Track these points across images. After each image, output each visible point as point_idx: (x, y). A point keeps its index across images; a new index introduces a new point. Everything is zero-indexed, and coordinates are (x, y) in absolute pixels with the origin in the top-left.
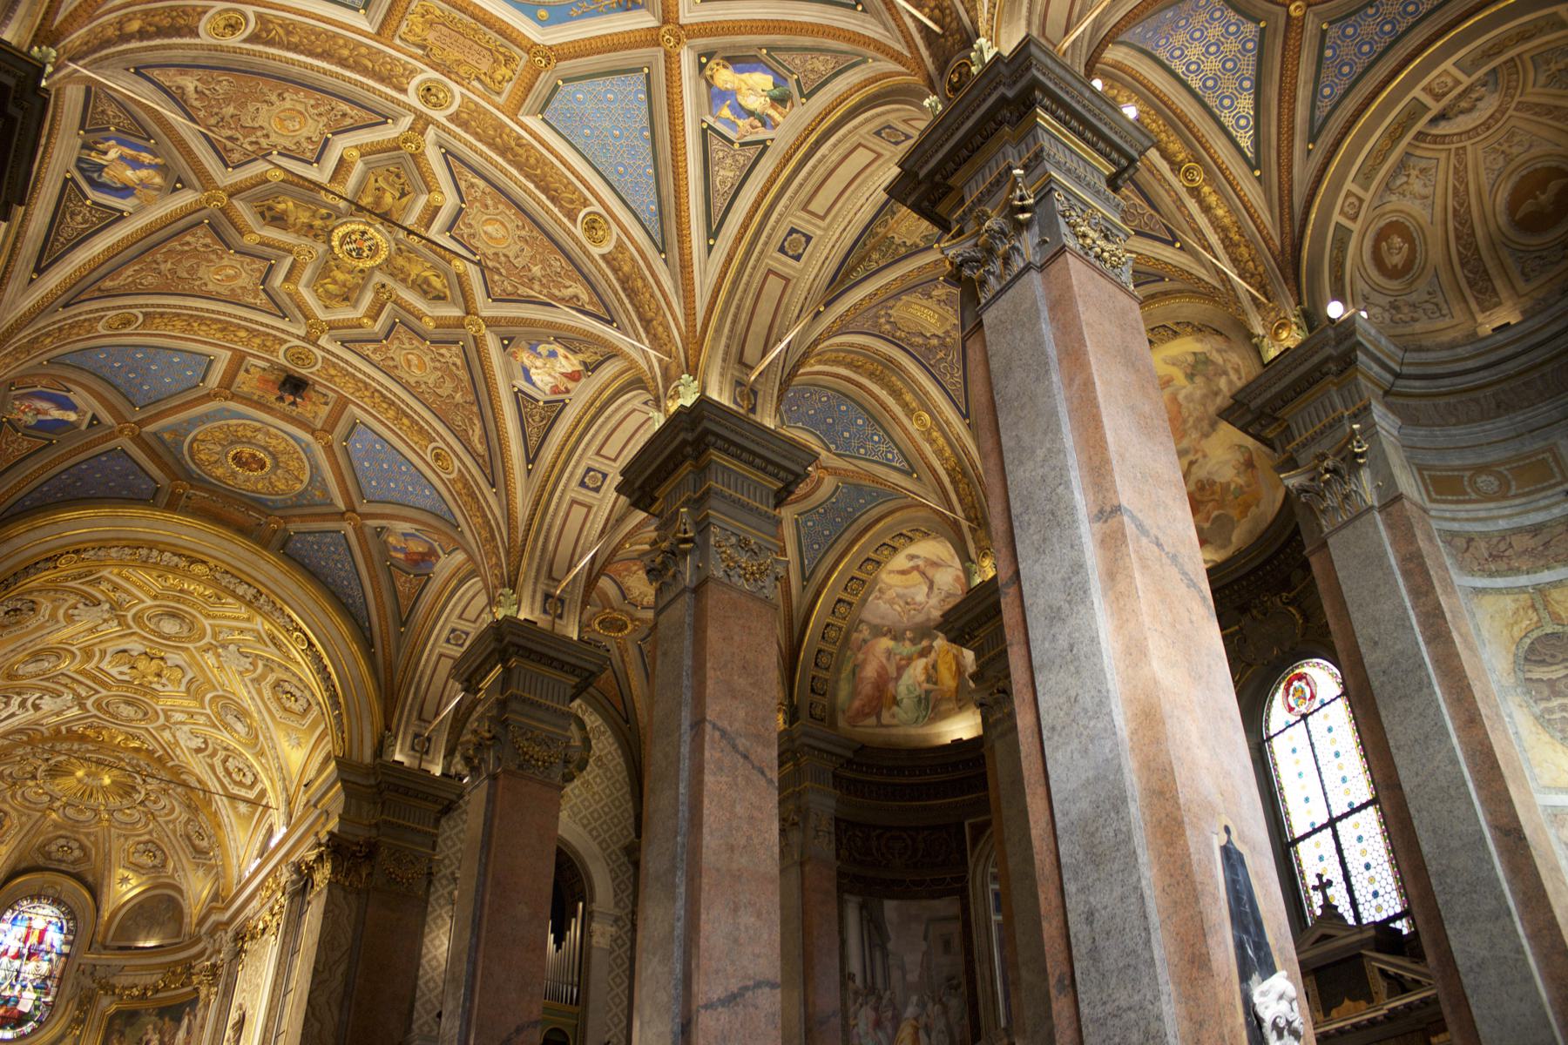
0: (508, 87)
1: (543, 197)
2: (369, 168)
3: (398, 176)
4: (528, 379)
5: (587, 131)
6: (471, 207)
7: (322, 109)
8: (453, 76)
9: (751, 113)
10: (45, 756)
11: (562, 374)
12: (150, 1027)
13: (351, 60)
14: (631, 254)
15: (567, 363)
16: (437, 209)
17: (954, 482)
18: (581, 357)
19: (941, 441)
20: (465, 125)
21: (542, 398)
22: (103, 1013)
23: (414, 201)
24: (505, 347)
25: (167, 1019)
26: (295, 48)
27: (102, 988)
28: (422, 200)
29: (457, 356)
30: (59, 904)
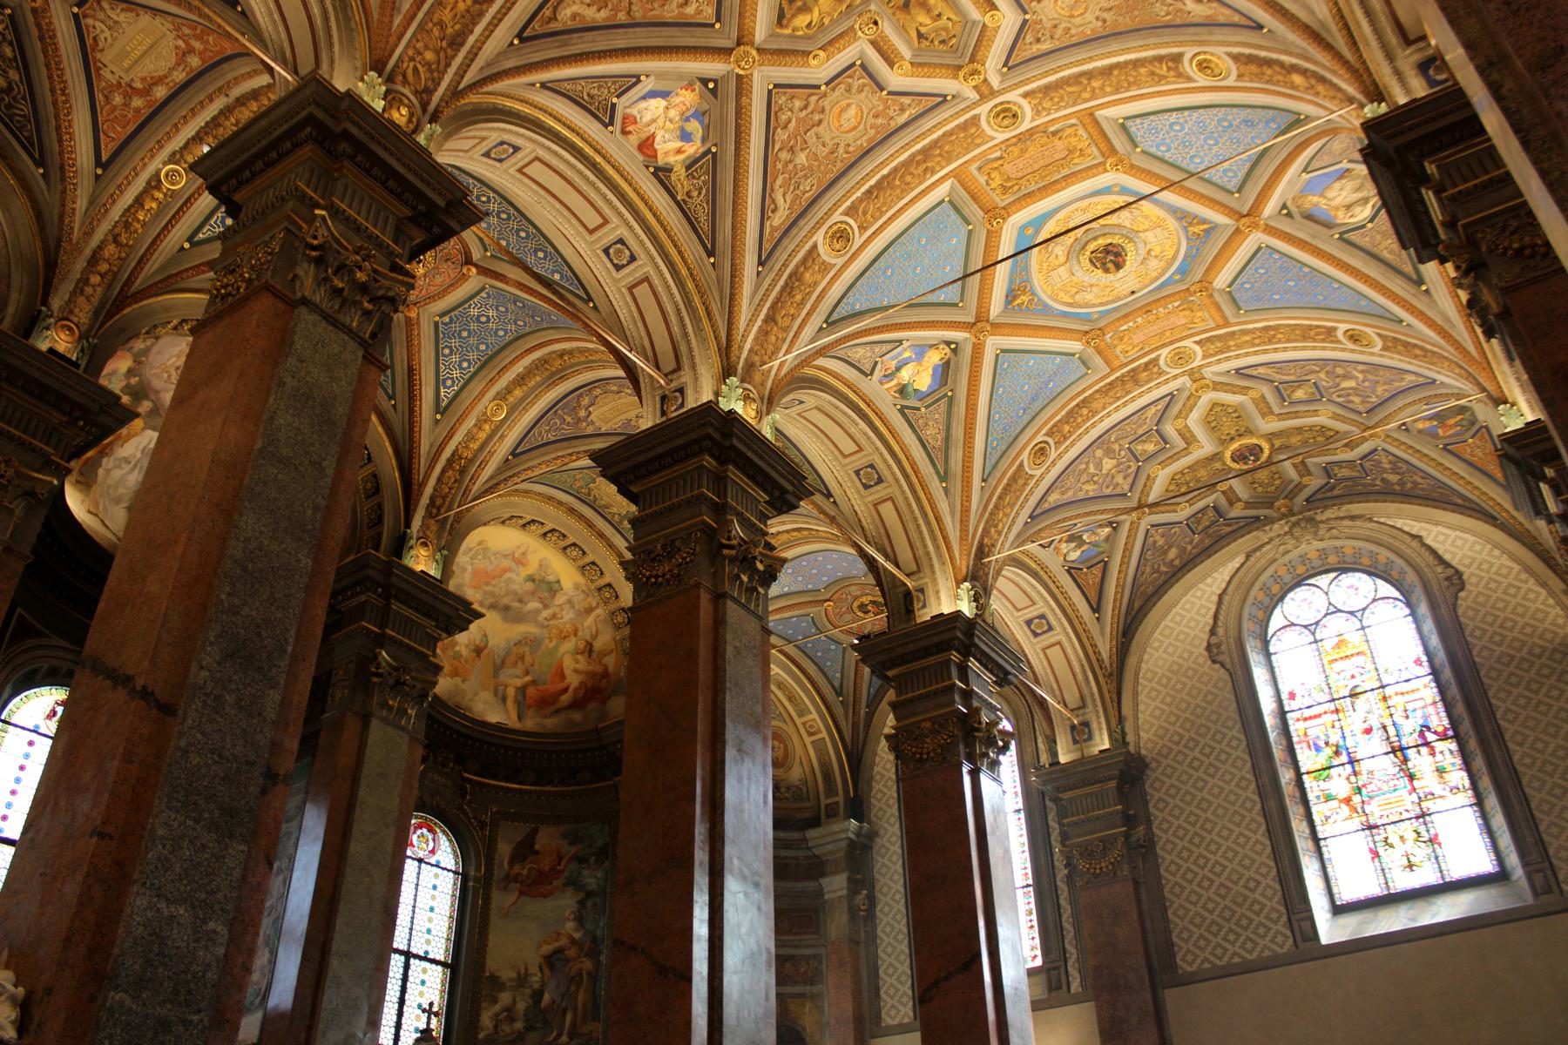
0: (982, 179)
1: (872, 182)
2: (966, 22)
3: (943, 42)
4: (653, 94)
5: (924, 241)
6: (880, 99)
7: (1059, 32)
8: (1014, 140)
9: (898, 369)
11: (653, 136)
13: (1085, 82)
14: (820, 282)
15: (669, 149)
16: (891, 64)
17: (450, 461)
18: (680, 172)
19: (482, 435)
20: (964, 127)
21: (621, 103)
23: (909, 43)
24: (705, 82)
26: (1137, 63)
28: (906, 53)
29: (699, 12)
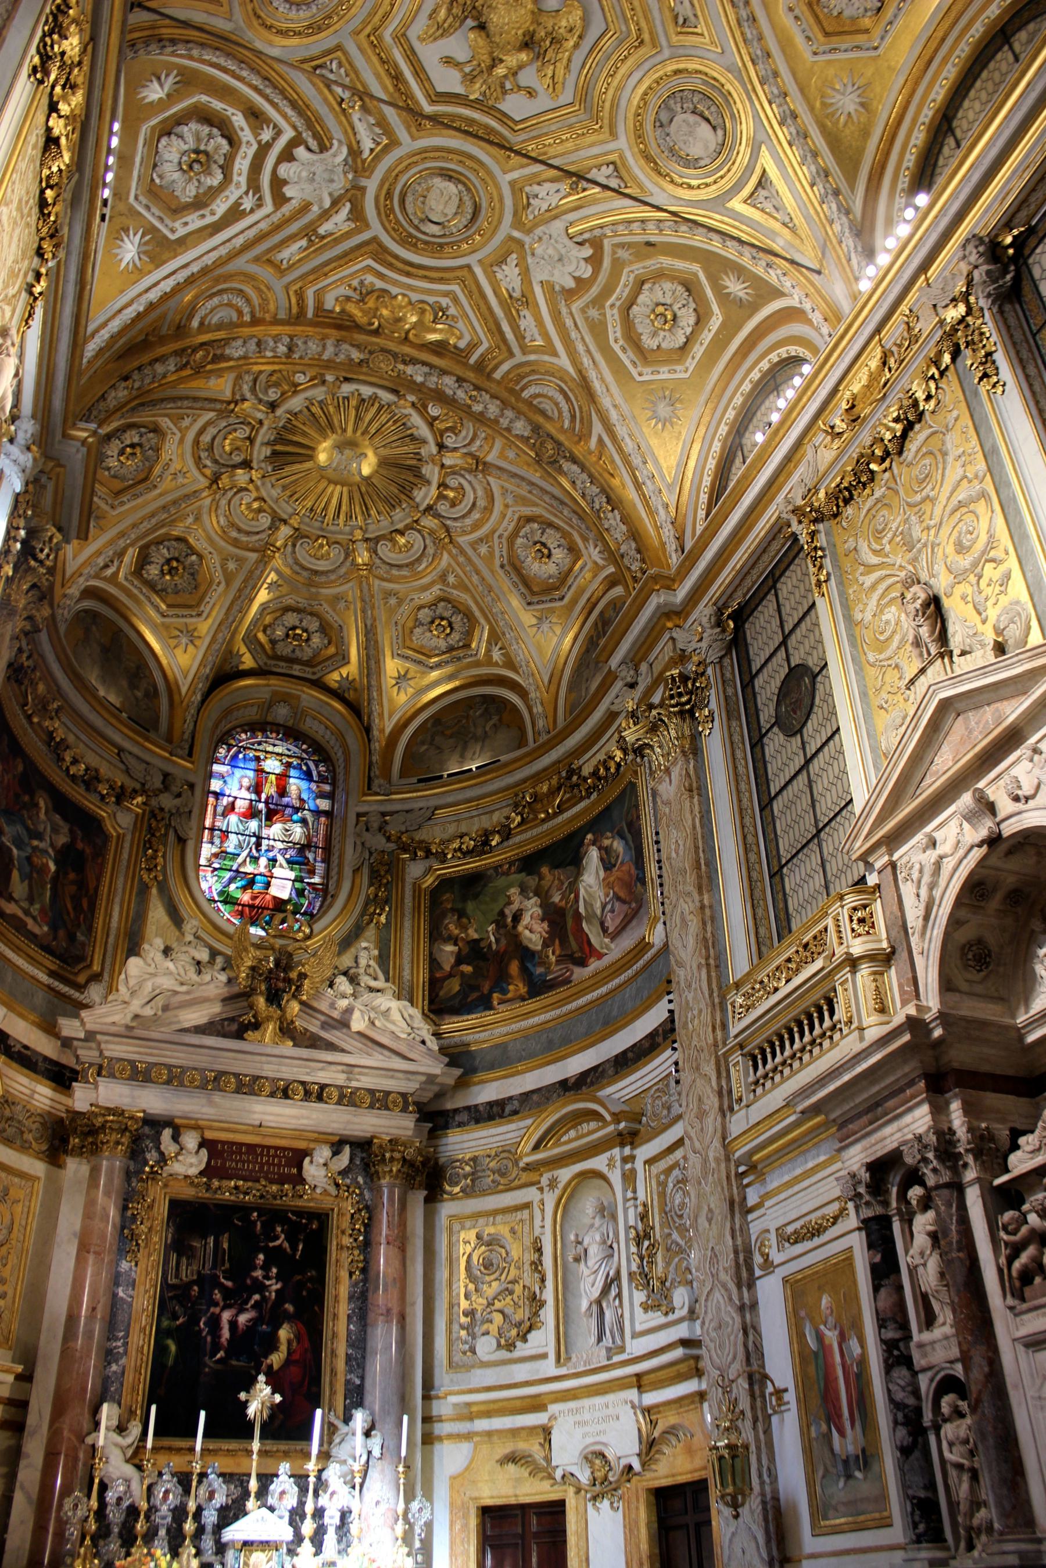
10: (273, 395)
12: (514, 891)
22: (416, 887)
25: (545, 870)
27: (405, 850)
30: (296, 739)
